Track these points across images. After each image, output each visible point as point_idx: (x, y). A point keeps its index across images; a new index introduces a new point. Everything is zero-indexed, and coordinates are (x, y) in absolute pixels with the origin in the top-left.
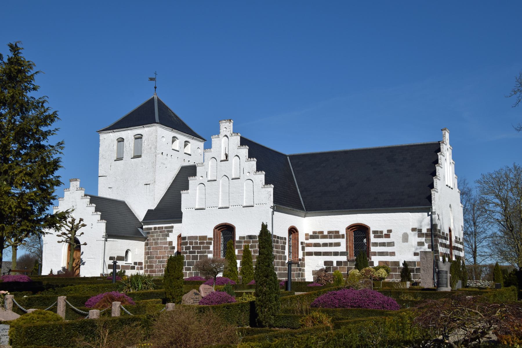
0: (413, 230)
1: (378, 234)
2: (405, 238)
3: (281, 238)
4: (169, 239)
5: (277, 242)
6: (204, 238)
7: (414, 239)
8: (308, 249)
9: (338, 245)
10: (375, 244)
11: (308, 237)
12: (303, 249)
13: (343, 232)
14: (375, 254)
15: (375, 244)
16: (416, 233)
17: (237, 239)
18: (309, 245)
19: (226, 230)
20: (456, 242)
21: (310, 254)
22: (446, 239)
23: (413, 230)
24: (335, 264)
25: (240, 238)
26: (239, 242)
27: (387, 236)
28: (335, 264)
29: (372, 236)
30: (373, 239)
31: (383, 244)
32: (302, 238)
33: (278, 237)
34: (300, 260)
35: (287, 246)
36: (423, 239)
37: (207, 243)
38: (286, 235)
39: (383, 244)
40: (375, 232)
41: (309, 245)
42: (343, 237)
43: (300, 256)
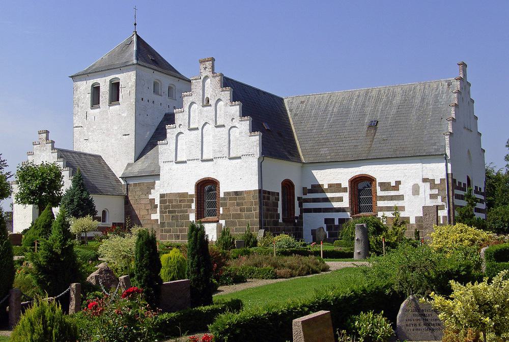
0: (425, 180)
1: (385, 186)
2: (416, 190)
3: (273, 193)
4: (151, 197)
5: (268, 198)
6: (184, 195)
7: (425, 189)
8: (306, 205)
9: (340, 199)
10: (383, 198)
11: (305, 191)
12: (300, 205)
13: (346, 184)
14: (382, 209)
15: (383, 198)
16: (428, 184)
17: (222, 195)
18: (307, 201)
19: (206, 187)
20: (476, 192)
21: (309, 211)
22: (464, 190)
23: (425, 180)
24: (336, 223)
25: (226, 194)
26: (224, 199)
27: (396, 188)
28: (336, 223)
29: (378, 188)
30: (380, 193)
31: (392, 198)
32: (298, 193)
33: (269, 193)
34: (297, 218)
35: (280, 203)
36: (436, 191)
37: (188, 201)
38: (279, 190)
39: (392, 198)
40: (381, 184)
41: (307, 201)
42: (345, 190)
43: (297, 213)
